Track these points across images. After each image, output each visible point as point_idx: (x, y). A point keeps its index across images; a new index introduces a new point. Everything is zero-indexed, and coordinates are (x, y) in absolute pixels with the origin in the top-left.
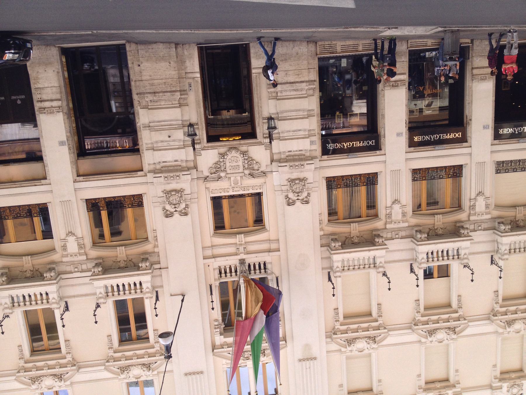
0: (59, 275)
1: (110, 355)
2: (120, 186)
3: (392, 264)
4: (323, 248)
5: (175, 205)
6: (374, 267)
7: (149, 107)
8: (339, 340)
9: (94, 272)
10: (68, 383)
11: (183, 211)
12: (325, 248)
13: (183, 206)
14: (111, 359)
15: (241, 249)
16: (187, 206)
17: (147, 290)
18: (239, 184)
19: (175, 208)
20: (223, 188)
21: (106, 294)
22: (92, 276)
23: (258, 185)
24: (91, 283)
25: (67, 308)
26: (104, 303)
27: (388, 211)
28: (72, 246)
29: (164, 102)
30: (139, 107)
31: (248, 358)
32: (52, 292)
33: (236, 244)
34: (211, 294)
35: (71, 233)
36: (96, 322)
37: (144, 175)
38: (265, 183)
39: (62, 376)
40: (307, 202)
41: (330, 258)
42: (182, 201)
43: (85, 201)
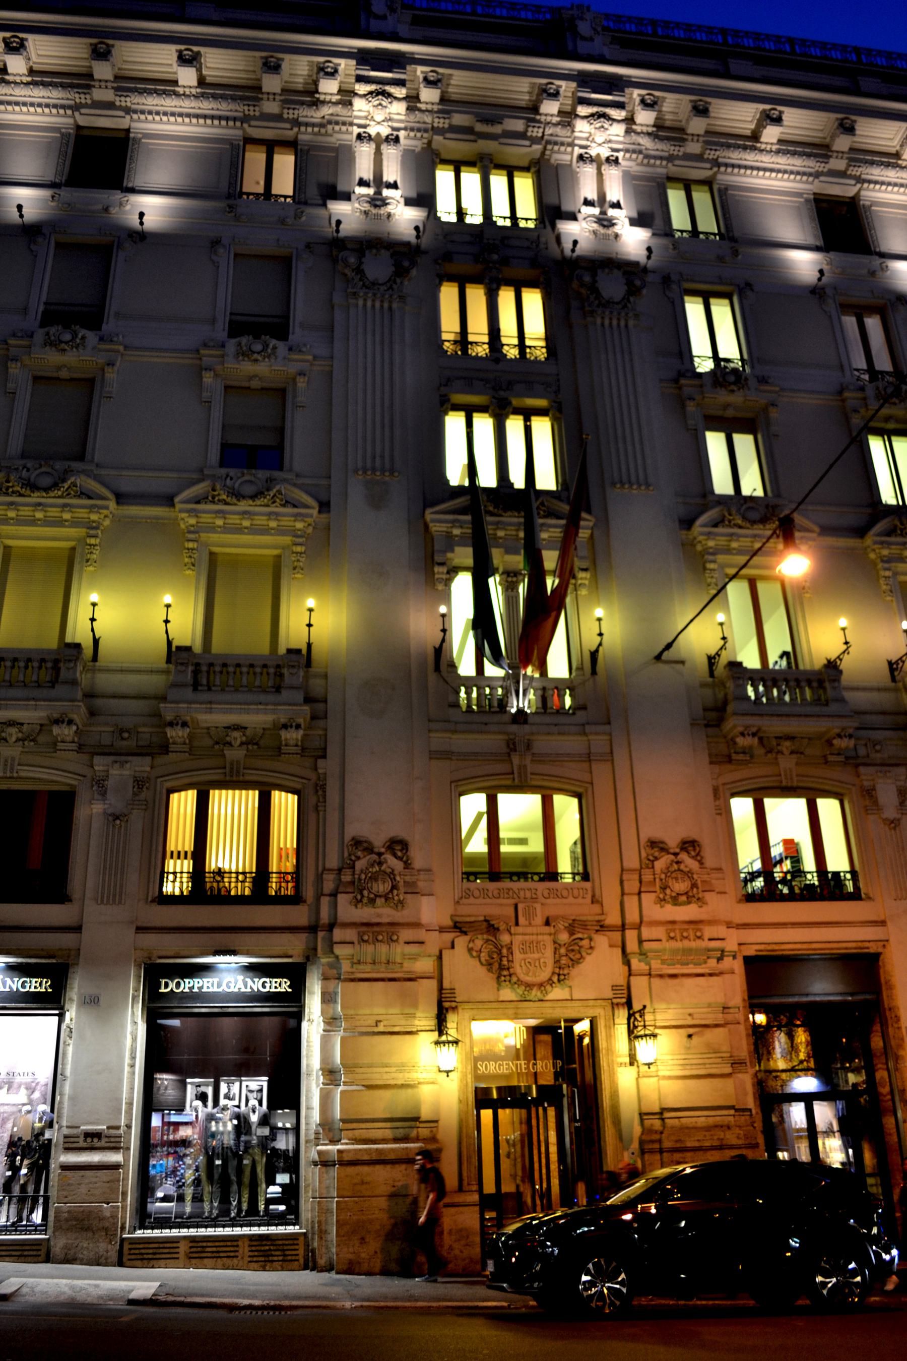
2: (794, 925)
5: (679, 870)
7: (732, 1112)
13: (659, 865)
19: (677, 863)
20: (558, 901)
23: (472, 900)
29: (699, 1125)
30: (754, 1112)
37: (742, 947)
42: (663, 876)
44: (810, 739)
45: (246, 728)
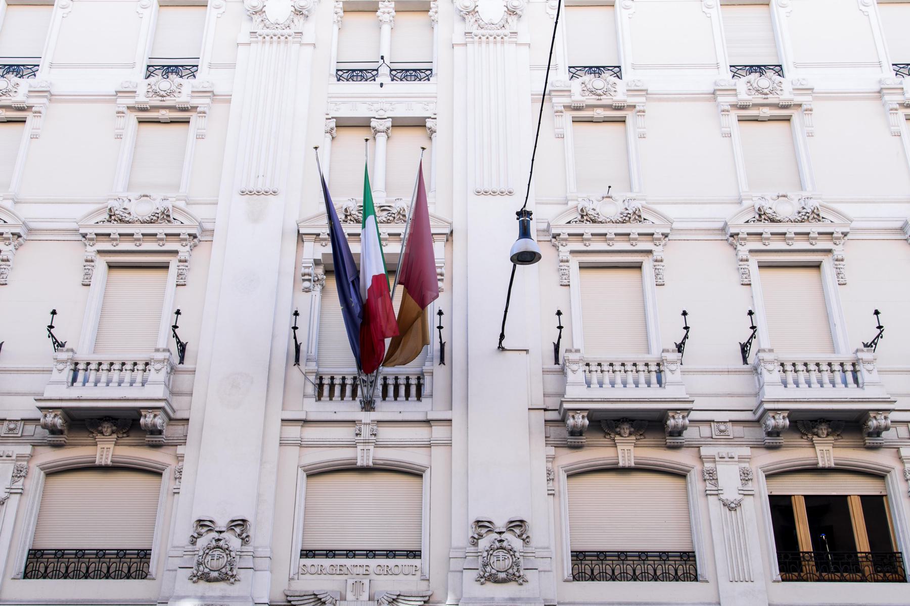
0: (758, 421)
1: (660, 248)
3: (40, 366)
4: (185, 417)
5: (501, 548)
6: (76, 364)
8: (186, 222)
9: (683, 417)
10: (746, 203)
11: (484, 531)
12: (179, 415)
13: (484, 544)
14: (659, 239)
15: (366, 432)
16: (475, 541)
17: (575, 367)
18: (350, 582)
19: (501, 541)
21: (662, 368)
22: (688, 410)
23: (308, 576)
24: (691, 395)
25: (744, 349)
26: (668, 351)
27: (19, 484)
28: (729, 478)
31: (382, 208)
32: (773, 384)
33: (376, 446)
34: (442, 345)
35: (731, 507)
36: (685, 313)
38: (291, 579)
39: (757, 216)
40: (201, 523)
41: (172, 393)
42: (485, 554)
43: (700, 578)
44: (649, 421)
45: (117, 419)
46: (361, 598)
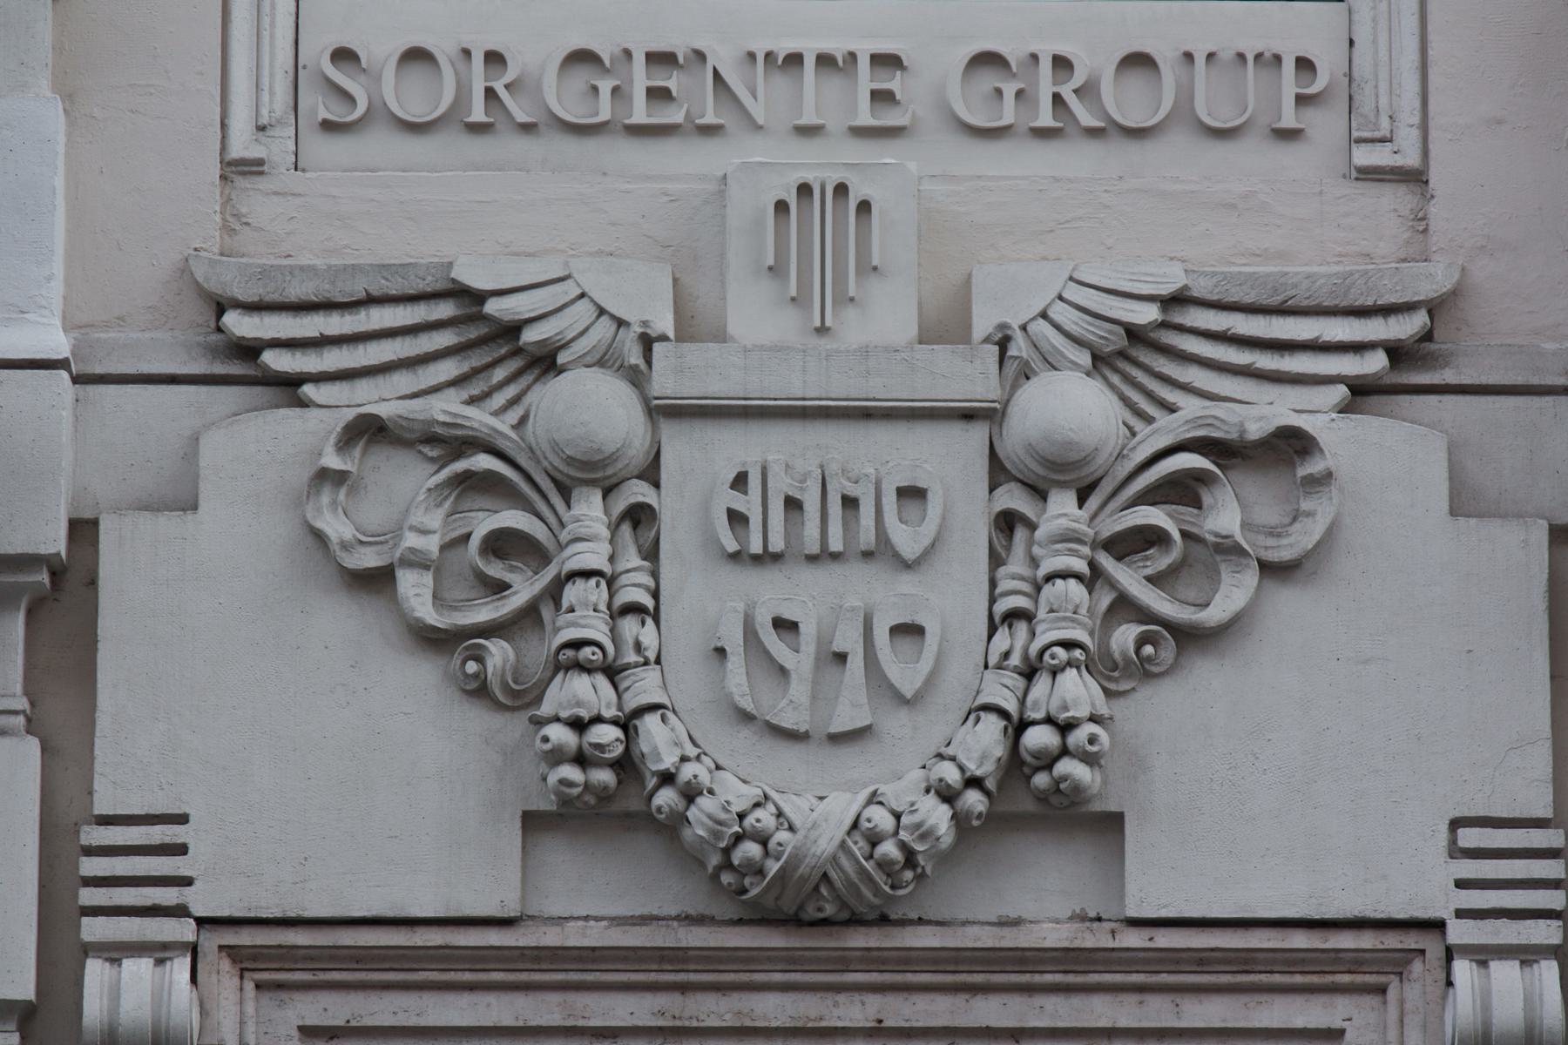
23: (380, 145)
46: (853, 330)
